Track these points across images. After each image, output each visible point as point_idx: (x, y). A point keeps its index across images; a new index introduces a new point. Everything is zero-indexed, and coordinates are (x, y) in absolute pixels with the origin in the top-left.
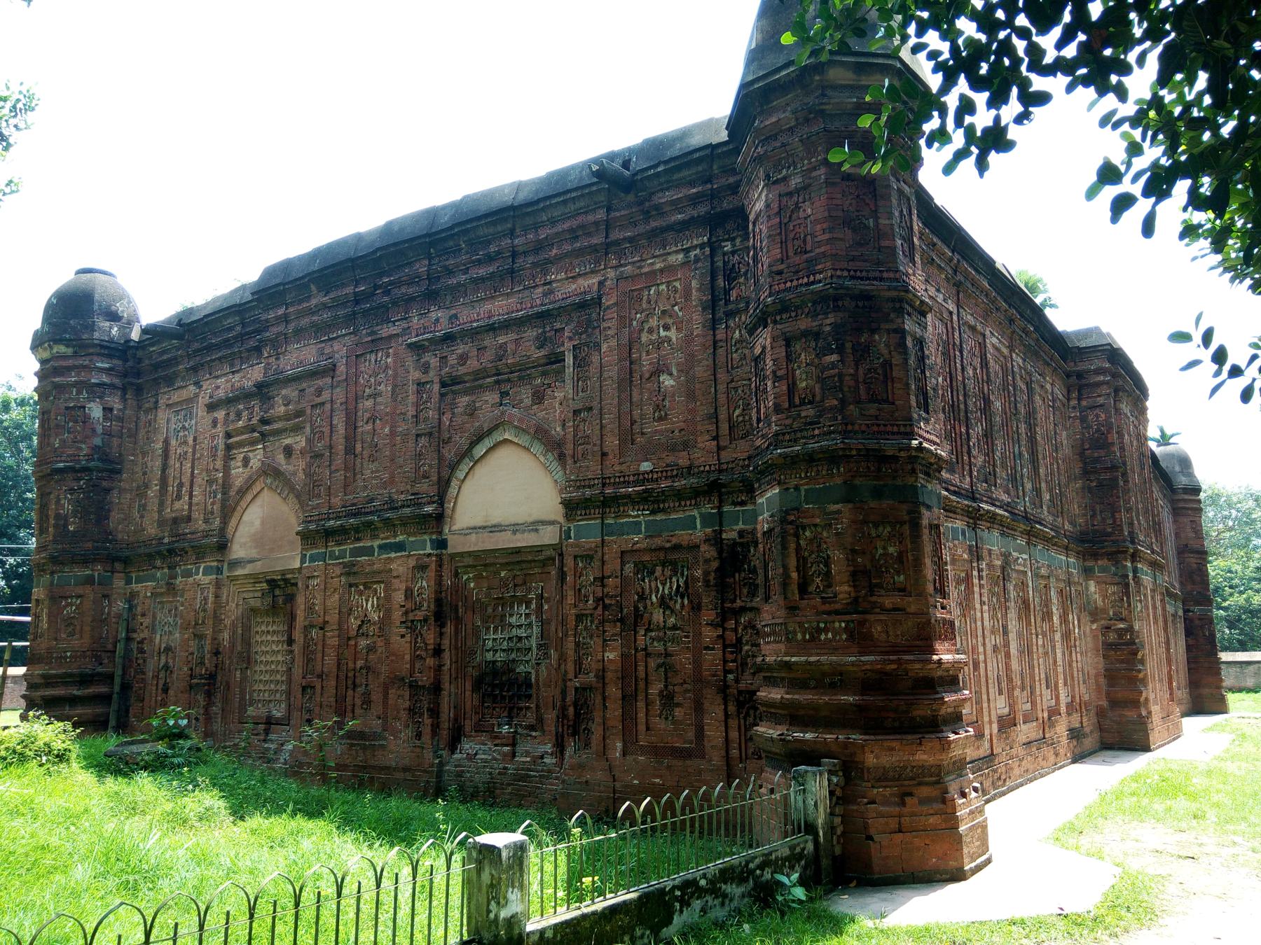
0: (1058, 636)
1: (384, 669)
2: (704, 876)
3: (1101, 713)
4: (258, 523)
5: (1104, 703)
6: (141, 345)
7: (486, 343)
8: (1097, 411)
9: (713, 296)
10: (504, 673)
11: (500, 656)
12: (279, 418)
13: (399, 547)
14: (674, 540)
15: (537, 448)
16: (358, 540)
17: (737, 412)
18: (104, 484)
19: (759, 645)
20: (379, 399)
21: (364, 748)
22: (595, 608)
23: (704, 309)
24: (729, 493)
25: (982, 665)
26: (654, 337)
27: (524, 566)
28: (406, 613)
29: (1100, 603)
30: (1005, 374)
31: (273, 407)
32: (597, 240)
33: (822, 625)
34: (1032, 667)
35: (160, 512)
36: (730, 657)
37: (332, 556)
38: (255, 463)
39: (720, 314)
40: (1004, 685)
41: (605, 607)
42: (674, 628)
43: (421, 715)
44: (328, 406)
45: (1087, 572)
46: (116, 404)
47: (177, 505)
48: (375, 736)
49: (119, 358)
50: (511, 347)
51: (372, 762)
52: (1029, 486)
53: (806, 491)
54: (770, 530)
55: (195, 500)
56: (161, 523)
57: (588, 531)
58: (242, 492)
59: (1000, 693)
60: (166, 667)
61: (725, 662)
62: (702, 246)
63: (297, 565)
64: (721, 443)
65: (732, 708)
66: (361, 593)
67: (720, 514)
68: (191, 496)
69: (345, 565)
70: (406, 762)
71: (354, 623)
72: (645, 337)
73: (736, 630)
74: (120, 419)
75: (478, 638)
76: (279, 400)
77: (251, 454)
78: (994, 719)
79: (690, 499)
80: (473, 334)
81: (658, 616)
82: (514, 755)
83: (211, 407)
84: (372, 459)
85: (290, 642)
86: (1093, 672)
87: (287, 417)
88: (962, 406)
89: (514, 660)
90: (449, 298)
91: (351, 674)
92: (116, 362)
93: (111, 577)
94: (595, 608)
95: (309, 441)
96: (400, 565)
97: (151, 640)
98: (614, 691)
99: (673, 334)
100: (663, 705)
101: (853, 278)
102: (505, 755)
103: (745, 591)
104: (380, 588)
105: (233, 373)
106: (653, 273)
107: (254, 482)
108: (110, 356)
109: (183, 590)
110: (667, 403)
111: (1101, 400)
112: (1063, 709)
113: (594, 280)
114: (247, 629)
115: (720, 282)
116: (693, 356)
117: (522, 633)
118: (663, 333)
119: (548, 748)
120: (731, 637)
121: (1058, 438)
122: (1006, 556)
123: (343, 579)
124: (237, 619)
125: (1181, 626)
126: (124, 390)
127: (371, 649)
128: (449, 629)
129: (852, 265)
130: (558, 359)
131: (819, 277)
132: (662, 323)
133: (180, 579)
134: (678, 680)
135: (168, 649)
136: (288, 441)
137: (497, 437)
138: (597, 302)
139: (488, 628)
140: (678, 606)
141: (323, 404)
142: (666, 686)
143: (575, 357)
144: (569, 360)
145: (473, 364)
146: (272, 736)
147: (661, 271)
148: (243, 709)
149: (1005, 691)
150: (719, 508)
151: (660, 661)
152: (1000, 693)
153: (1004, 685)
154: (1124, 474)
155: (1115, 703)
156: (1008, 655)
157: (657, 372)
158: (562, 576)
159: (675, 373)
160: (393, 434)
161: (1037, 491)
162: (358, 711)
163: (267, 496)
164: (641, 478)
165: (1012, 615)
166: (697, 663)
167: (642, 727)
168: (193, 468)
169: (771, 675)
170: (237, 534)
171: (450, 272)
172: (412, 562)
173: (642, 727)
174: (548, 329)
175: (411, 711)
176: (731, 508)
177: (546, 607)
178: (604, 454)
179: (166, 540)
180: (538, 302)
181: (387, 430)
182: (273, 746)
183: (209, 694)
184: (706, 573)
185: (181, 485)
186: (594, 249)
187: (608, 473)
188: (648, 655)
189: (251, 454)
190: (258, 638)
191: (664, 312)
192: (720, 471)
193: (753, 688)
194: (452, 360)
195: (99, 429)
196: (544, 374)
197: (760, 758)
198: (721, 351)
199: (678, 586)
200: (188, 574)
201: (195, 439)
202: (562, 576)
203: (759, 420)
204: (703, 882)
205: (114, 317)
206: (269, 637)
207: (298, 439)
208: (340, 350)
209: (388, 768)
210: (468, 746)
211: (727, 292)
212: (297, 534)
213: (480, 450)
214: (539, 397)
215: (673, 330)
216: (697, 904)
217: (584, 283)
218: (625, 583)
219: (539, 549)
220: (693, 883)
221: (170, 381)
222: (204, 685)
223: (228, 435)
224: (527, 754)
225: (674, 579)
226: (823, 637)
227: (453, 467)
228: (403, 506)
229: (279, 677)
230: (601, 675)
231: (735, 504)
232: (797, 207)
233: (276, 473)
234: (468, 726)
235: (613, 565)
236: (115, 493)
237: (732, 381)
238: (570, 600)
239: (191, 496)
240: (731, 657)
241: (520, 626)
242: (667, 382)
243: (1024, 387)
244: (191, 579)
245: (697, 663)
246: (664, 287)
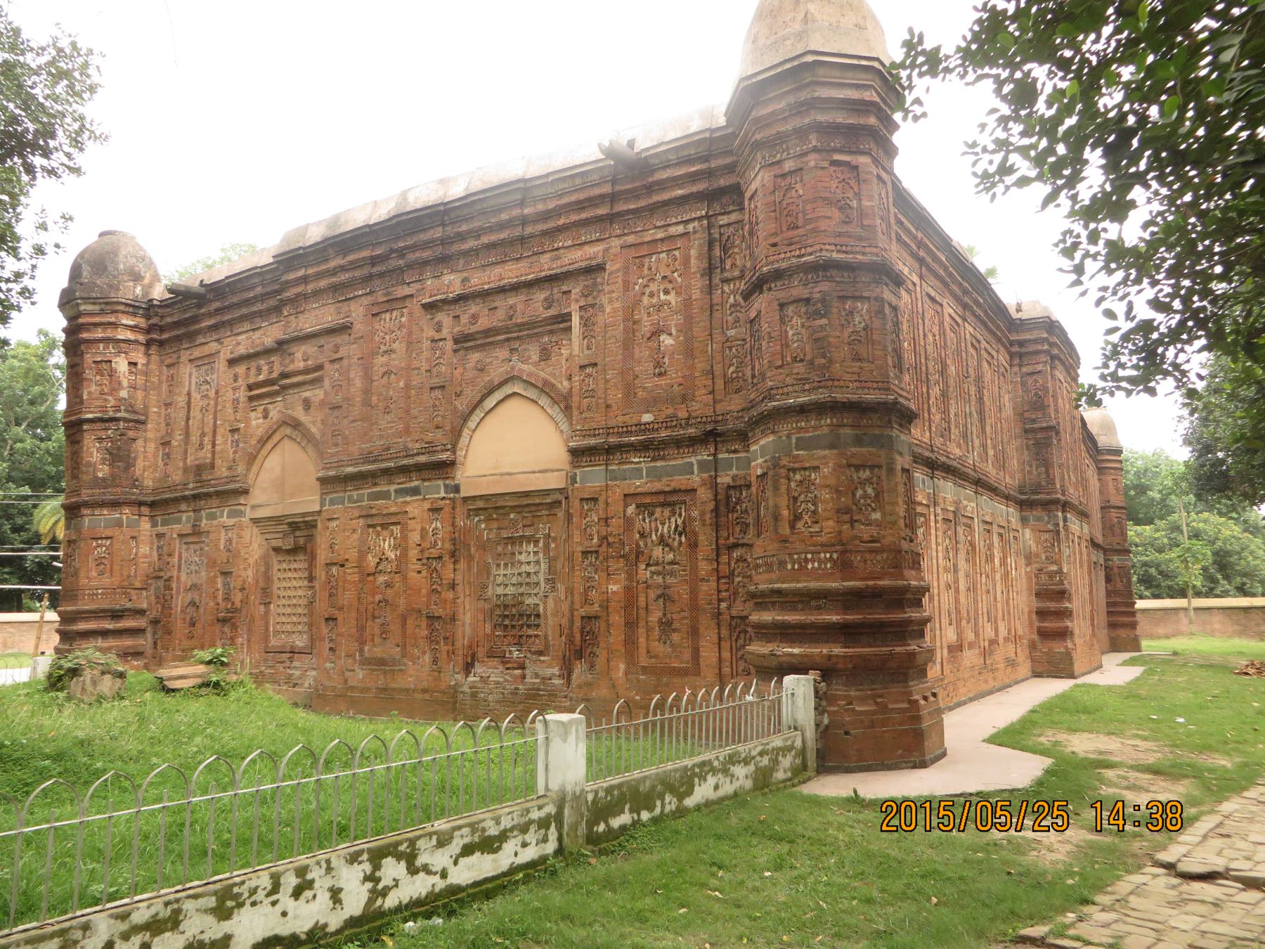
0: (998, 576)
1: (402, 602)
2: (717, 758)
3: (1033, 646)
4: (278, 470)
5: (1035, 637)
6: (164, 304)
7: (496, 304)
8: (1035, 377)
9: (710, 264)
10: (514, 606)
11: (510, 590)
13: (415, 491)
14: (674, 485)
15: (544, 401)
16: (375, 484)
17: (732, 369)
18: (131, 434)
19: (750, 576)
20: (393, 356)
21: (385, 672)
22: (600, 546)
23: (702, 275)
24: (723, 442)
25: (936, 598)
26: (654, 300)
27: (533, 508)
28: (422, 551)
29: (1034, 548)
30: (959, 342)
31: (292, 361)
32: (602, 211)
33: (809, 556)
34: (976, 602)
36: (723, 587)
37: (350, 499)
38: (274, 414)
39: (716, 280)
40: (953, 616)
41: (609, 544)
42: (672, 563)
43: (438, 643)
44: (345, 362)
45: (1024, 520)
46: (141, 360)
47: (201, 454)
48: (394, 662)
49: (143, 316)
50: (520, 307)
51: (393, 685)
52: (977, 442)
53: (797, 439)
54: (764, 475)
55: (218, 448)
56: (186, 470)
57: (594, 477)
58: (263, 441)
59: (950, 624)
60: (192, 603)
61: (719, 591)
62: (700, 219)
63: (317, 508)
64: (718, 397)
65: (725, 633)
66: (378, 535)
67: (716, 460)
68: (214, 445)
70: (425, 684)
71: (371, 560)
72: (646, 300)
73: (729, 564)
74: (146, 374)
75: (489, 573)
76: (299, 355)
78: (945, 645)
79: (688, 446)
80: (484, 295)
81: (658, 552)
82: (524, 677)
83: (232, 362)
84: (387, 411)
85: (311, 578)
86: (1026, 610)
87: (306, 371)
88: (924, 368)
89: (522, 594)
90: (461, 262)
91: (370, 607)
92: (138, 319)
93: (138, 521)
94: (600, 546)
95: (326, 393)
96: (416, 508)
97: (178, 578)
98: (617, 619)
99: (672, 298)
100: (663, 632)
101: (838, 251)
102: (516, 677)
103: (738, 529)
104: (396, 530)
105: (253, 330)
106: (655, 241)
107: (274, 432)
108: (134, 314)
110: (666, 360)
111: (1040, 367)
112: (1001, 641)
113: (599, 248)
114: (268, 567)
115: (717, 252)
116: (692, 318)
117: (531, 569)
118: (663, 297)
119: (556, 671)
120: (724, 569)
121: (1004, 400)
122: (957, 503)
123: (362, 521)
125: (1102, 574)
126: (148, 344)
127: (388, 585)
128: (462, 565)
129: (837, 240)
130: (566, 318)
131: (809, 250)
132: (662, 287)
133: (204, 521)
134: (675, 608)
135: (194, 587)
136: (307, 394)
137: (508, 389)
138: (600, 268)
139: (498, 565)
140: (676, 544)
141: (341, 359)
142: (665, 615)
143: (581, 317)
144: (576, 320)
145: (484, 323)
146: (296, 664)
147: (662, 240)
148: (266, 638)
149: (954, 622)
150: (715, 455)
151: (659, 592)
152: (950, 624)
153: (953, 616)
154: (1058, 433)
155: (1044, 634)
156: (957, 591)
157: (656, 333)
158: (569, 517)
159: (674, 332)
160: (408, 387)
161: (984, 446)
162: (377, 640)
163: (287, 444)
164: (643, 428)
165: (962, 555)
166: (694, 593)
167: (642, 651)
168: (215, 419)
169: (762, 600)
171: (461, 237)
172: (427, 505)
173: (642, 651)
174: (555, 290)
175: (431, 639)
176: (726, 455)
177: (553, 546)
178: (608, 406)
179: (191, 486)
180: (546, 267)
181: (402, 384)
182: (297, 673)
184: (702, 514)
185: (203, 434)
186: (600, 219)
187: (612, 423)
188: (648, 587)
191: (664, 277)
192: (716, 422)
193: (744, 613)
194: (464, 319)
195: (125, 383)
196: (551, 332)
197: (749, 674)
198: (717, 315)
199: (677, 526)
200: (212, 517)
201: (217, 392)
202: (569, 517)
203: (753, 376)
204: (716, 763)
205: (137, 278)
206: (290, 575)
207: (317, 392)
208: (357, 311)
209: (407, 690)
210: (479, 669)
211: (722, 261)
212: (318, 479)
213: (490, 402)
214: (545, 355)
215: (673, 294)
216: (711, 780)
217: (591, 250)
218: (629, 522)
219: (547, 492)
220: (710, 762)
221: (191, 336)
223: (250, 388)
224: (537, 676)
225: (673, 520)
226: (810, 566)
227: (466, 418)
228: (418, 454)
230: (605, 606)
231: (728, 452)
232: (790, 188)
233: (296, 425)
234: (481, 653)
235: (616, 508)
236: (140, 442)
237: (727, 340)
238: (577, 539)
239: (214, 445)
240: (723, 587)
241: (528, 563)
242: (667, 341)
243: (974, 352)
244: (215, 522)
245: (694, 593)
246: (664, 255)
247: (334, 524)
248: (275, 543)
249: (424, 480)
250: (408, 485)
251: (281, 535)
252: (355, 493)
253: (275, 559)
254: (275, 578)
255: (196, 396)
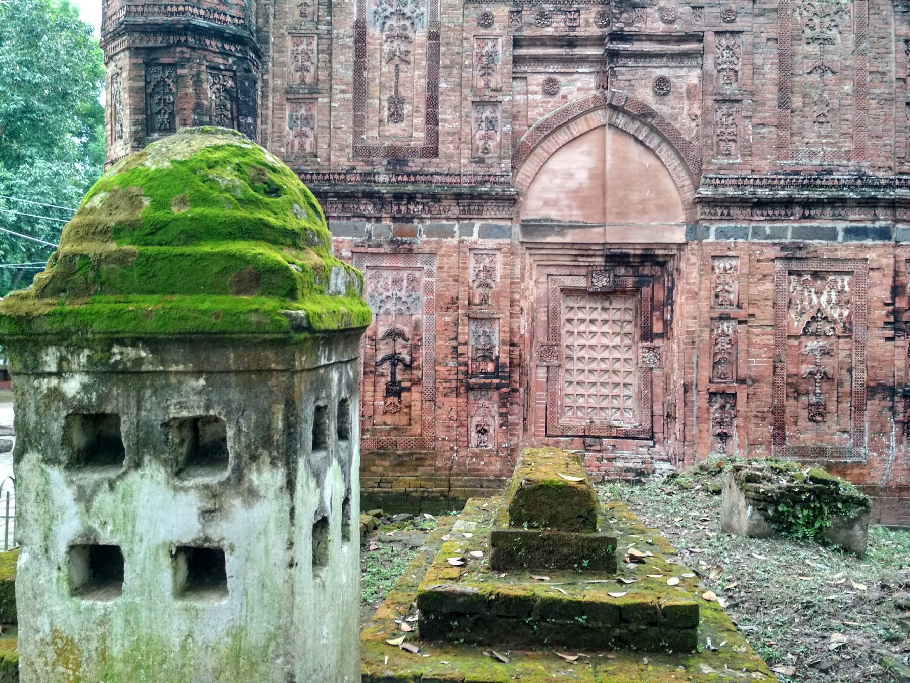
12: (650, 38)
13: (884, 234)
16: (810, 217)
20: (829, 47)
35: (357, 134)
56: (362, 152)
58: (548, 130)
60: (394, 359)
69: (783, 248)
77: (561, 79)
96: (877, 253)
109: (432, 254)
114: (553, 315)
123: (779, 265)
124: (538, 300)
135: (394, 335)
136: (664, 72)
170: (537, 188)
181: (848, 87)
183: (505, 401)
189: (561, 79)
190: (569, 327)
201: (434, 37)
206: (593, 328)
207: (683, 72)
222: (498, 387)
223: (517, 43)
229: (616, 379)
239: (432, 119)
247: (727, 263)
248: (569, 282)
249: (897, 221)
250: (869, 225)
251: (584, 271)
252: (768, 227)
253: (564, 304)
254: (563, 332)
255: (373, 31)
